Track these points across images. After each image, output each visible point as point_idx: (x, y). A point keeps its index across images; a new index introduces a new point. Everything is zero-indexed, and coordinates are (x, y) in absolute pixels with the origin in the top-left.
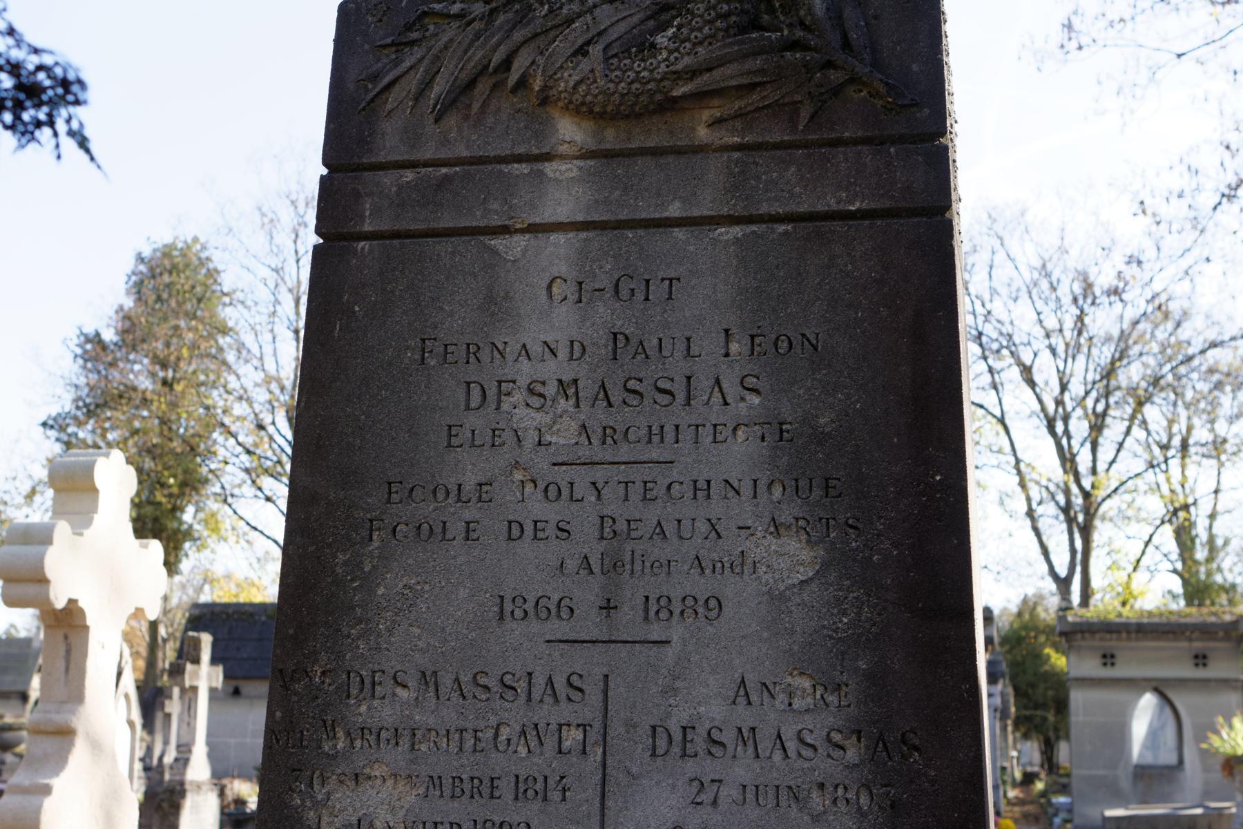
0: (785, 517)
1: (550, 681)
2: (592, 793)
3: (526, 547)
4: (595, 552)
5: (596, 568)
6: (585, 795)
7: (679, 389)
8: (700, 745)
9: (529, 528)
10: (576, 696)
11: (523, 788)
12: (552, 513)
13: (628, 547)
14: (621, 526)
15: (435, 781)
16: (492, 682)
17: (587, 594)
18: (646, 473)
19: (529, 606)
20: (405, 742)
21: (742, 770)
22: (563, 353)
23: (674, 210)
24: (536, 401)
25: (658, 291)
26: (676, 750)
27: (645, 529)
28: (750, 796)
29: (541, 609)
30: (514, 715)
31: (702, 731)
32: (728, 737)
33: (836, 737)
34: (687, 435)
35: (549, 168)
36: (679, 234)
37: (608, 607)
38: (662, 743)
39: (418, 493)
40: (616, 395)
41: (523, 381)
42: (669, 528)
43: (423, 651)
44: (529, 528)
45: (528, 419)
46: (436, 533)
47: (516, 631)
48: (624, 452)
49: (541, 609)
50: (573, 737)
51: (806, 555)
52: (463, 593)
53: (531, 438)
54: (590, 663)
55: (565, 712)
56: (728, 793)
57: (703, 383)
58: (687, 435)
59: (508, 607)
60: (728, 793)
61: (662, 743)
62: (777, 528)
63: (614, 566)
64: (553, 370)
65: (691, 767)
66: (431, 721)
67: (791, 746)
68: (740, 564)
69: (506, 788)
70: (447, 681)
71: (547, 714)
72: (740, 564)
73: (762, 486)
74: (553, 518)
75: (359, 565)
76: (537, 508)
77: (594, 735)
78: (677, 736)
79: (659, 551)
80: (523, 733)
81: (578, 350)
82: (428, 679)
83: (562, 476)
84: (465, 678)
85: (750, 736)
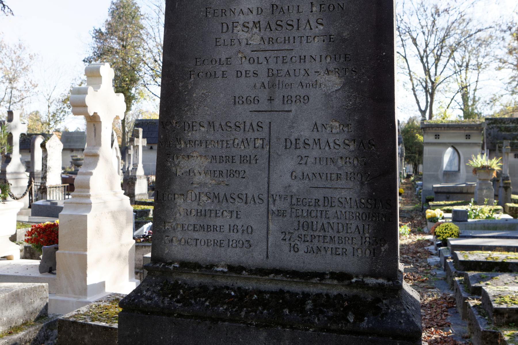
0: (331, 68)
1: (251, 125)
2: (266, 161)
3: (243, 80)
4: (266, 80)
5: (267, 86)
6: (263, 162)
7: (295, 24)
8: (301, 145)
9: (244, 73)
10: (260, 129)
12: (251, 68)
13: (277, 79)
14: (275, 72)
15: (214, 158)
16: (232, 125)
17: (264, 95)
18: (283, 53)
19: (244, 100)
20: (204, 145)
21: (315, 153)
22: (255, 12)
24: (246, 29)
26: (293, 146)
27: (283, 73)
28: (318, 161)
29: (248, 101)
30: (239, 136)
31: (302, 140)
32: (311, 142)
33: (347, 142)
34: (298, 40)
37: (271, 100)
38: (289, 144)
39: (206, 62)
40: (273, 27)
41: (241, 22)
42: (292, 72)
43: (209, 115)
44: (244, 73)
45: (243, 35)
47: (240, 108)
48: (276, 46)
49: (248, 101)
50: (259, 143)
51: (338, 81)
52: (222, 95)
53: (244, 42)
54: (264, 118)
55: (256, 135)
56: (311, 160)
57: (303, 22)
58: (298, 40)
59: (237, 100)
60: (311, 160)
61: (289, 144)
62: (328, 72)
64: (252, 18)
65: (298, 152)
66: (212, 138)
67: (332, 145)
68: (315, 84)
69: (237, 159)
70: (217, 125)
71: (250, 135)
72: (315, 84)
73: (323, 57)
74: (252, 70)
75: (187, 87)
76: (247, 66)
77: (266, 142)
78: (294, 142)
79: (288, 80)
80: (243, 141)
82: (211, 124)
83: (255, 55)
84: (223, 124)
85: (318, 142)
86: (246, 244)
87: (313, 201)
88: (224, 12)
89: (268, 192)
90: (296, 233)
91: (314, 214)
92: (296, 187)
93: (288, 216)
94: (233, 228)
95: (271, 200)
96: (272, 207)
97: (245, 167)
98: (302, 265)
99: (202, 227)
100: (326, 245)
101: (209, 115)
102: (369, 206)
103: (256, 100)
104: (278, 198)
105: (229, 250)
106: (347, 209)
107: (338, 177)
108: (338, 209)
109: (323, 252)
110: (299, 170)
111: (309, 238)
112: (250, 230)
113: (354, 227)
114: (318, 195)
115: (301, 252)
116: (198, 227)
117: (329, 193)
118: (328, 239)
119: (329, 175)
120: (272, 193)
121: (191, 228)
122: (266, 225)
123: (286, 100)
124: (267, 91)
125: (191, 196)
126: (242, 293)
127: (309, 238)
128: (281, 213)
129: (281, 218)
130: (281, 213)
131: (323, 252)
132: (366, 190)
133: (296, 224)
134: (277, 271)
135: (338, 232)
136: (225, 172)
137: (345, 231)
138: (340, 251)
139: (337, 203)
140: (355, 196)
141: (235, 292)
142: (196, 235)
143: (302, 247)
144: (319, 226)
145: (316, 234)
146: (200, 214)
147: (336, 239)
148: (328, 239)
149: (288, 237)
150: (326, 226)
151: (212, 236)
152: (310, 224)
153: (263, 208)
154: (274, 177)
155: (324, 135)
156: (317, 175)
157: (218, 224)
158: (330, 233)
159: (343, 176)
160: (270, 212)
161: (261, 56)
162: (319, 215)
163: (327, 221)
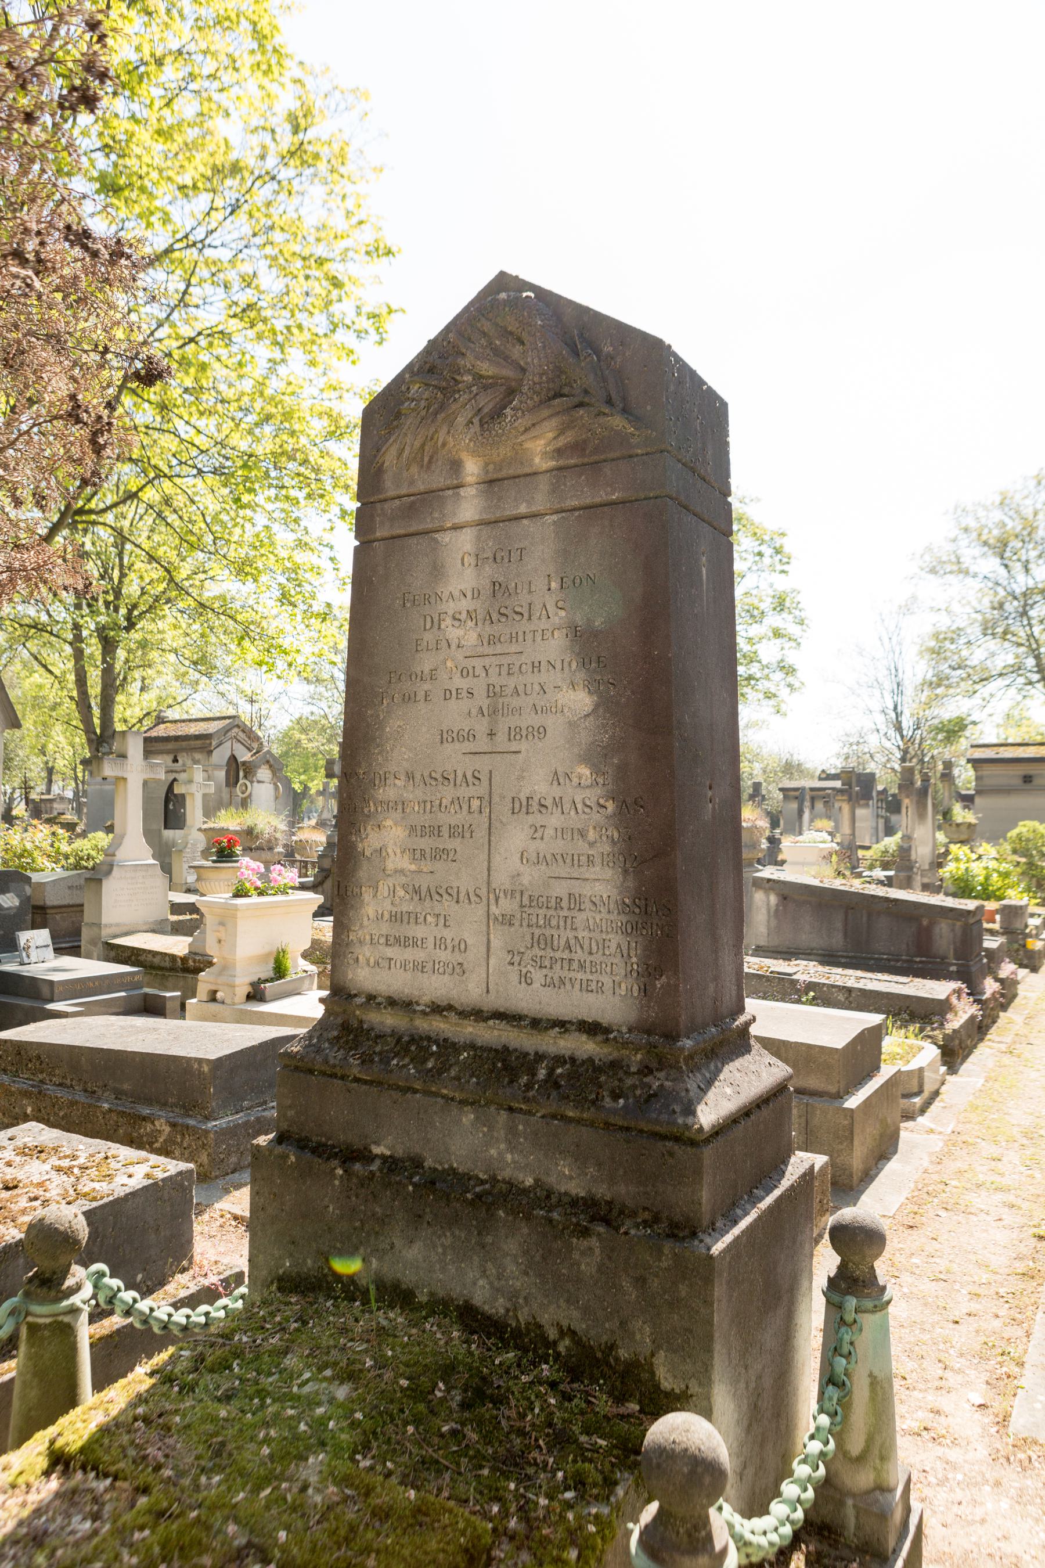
1: (465, 776)
4: (485, 703)
5: (486, 713)
6: (481, 834)
8: (535, 807)
9: (454, 693)
10: (477, 782)
11: (455, 832)
13: (501, 700)
14: (497, 689)
16: (438, 776)
17: (481, 727)
19: (455, 735)
20: (400, 807)
22: (469, 595)
23: (523, 509)
24: (457, 623)
25: (515, 556)
26: (524, 810)
27: (509, 691)
28: (559, 834)
30: (448, 793)
31: (536, 799)
32: (548, 803)
33: (602, 801)
35: (462, 492)
36: (525, 522)
37: (491, 734)
38: (517, 806)
39: (403, 678)
40: (495, 616)
41: (450, 613)
42: (521, 689)
43: (407, 760)
44: (454, 693)
45: (454, 633)
46: (409, 699)
47: (449, 748)
50: (476, 803)
52: (424, 729)
54: (483, 764)
55: (472, 791)
56: (549, 832)
59: (445, 736)
60: (549, 832)
61: (517, 806)
63: (494, 712)
64: (465, 605)
65: (530, 819)
66: (411, 797)
67: (579, 806)
70: (418, 776)
71: (464, 792)
73: (566, 664)
74: (465, 687)
75: (378, 716)
76: (458, 682)
77: (485, 803)
78: (524, 803)
79: (515, 702)
80: (452, 802)
81: (477, 594)
82: (410, 776)
84: (426, 774)
85: (558, 803)
86: (458, 970)
87: (553, 900)
88: (427, 599)
89: (489, 883)
90: (529, 954)
91: (554, 922)
92: (530, 876)
93: (517, 924)
94: (440, 943)
95: (492, 896)
96: (493, 908)
97: (455, 844)
98: (538, 1007)
99: (397, 940)
100: (572, 974)
101: (407, 760)
102: (637, 910)
103: (471, 736)
104: (502, 895)
105: (434, 978)
106: (604, 915)
107: (590, 861)
108: (590, 914)
109: (568, 986)
110: (533, 846)
111: (547, 963)
112: (463, 946)
113: (613, 945)
114: (560, 889)
115: (536, 985)
116: (392, 939)
117: (577, 888)
118: (575, 965)
119: (576, 858)
120: (494, 886)
121: (382, 940)
122: (485, 939)
123: (515, 733)
124: (485, 721)
125: (384, 889)
126: (449, 1047)
127: (547, 963)
128: (507, 920)
129: (506, 927)
130: (507, 920)
131: (568, 986)
132: (630, 884)
133: (528, 937)
134: (500, 1016)
135: (591, 953)
136: (428, 851)
137: (601, 952)
138: (593, 986)
139: (587, 905)
140: (615, 894)
141: (438, 1046)
142: (389, 952)
143: (538, 976)
144: (563, 942)
145: (558, 955)
146: (396, 918)
147: (588, 964)
148: (575, 965)
149: (517, 959)
150: (572, 942)
151: (409, 954)
152: (549, 939)
153: (481, 911)
154: (497, 859)
155: (568, 791)
156: (559, 857)
157: (419, 936)
158: (579, 955)
159: (598, 860)
160: (492, 917)
161: (478, 663)
162: (562, 923)
163: (574, 933)
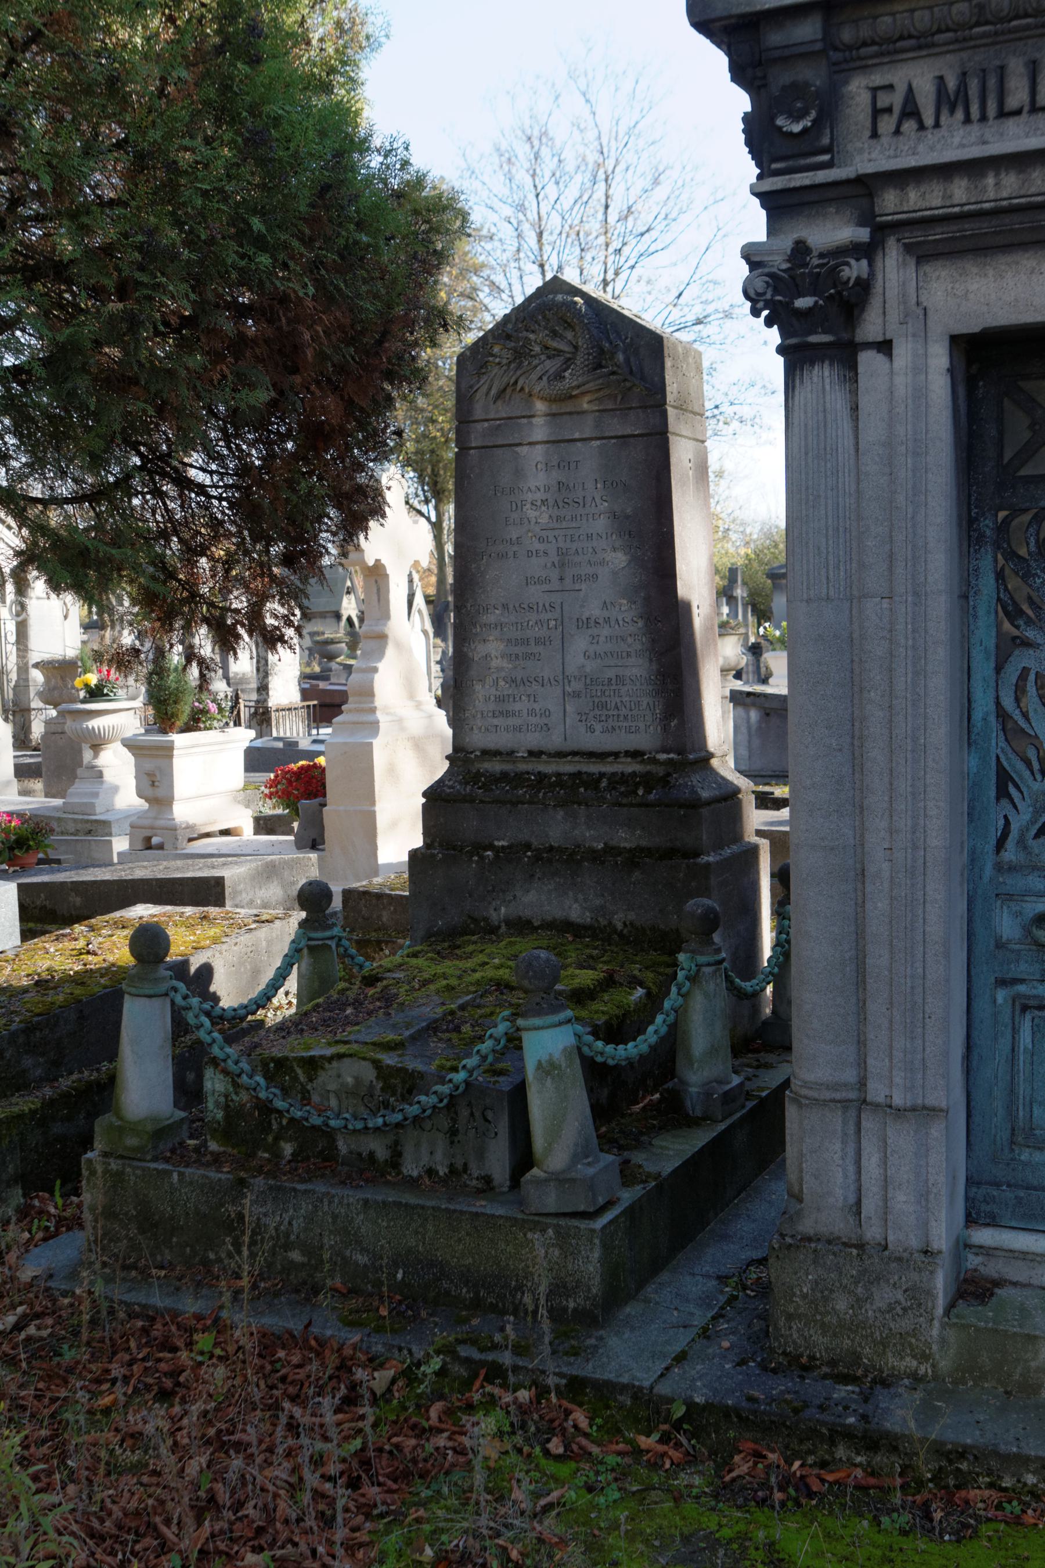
0: (617, 545)
2: (559, 642)
3: (534, 560)
4: (556, 560)
7: (581, 501)
8: (592, 624)
11: (538, 641)
12: (541, 547)
15: (509, 641)
17: (554, 575)
18: (571, 532)
21: (606, 631)
23: (577, 436)
25: (573, 466)
29: (540, 581)
30: (533, 617)
32: (601, 621)
34: (584, 518)
35: (535, 420)
36: (579, 444)
40: (561, 504)
45: (532, 514)
46: (502, 556)
47: (532, 589)
48: (564, 525)
49: (540, 581)
50: (552, 623)
51: (624, 558)
53: (533, 520)
55: (549, 615)
56: (602, 639)
57: (589, 499)
58: (584, 518)
60: (602, 639)
62: (614, 549)
63: (562, 565)
64: (539, 496)
65: (590, 631)
68: (603, 563)
69: (532, 642)
70: (511, 607)
71: (545, 616)
72: (603, 563)
76: (537, 546)
81: (547, 488)
82: (505, 607)
83: (544, 534)
85: (607, 620)
88: (512, 490)
90: (592, 714)
92: (590, 666)
94: (532, 712)
96: (567, 688)
97: (540, 649)
99: (501, 713)
103: (547, 580)
113: (645, 704)
114: (610, 673)
115: (597, 733)
125: (489, 681)
126: (542, 777)
128: (577, 695)
130: (577, 695)
132: (654, 667)
134: (574, 753)
139: (628, 681)
142: (496, 722)
143: (598, 727)
145: (611, 713)
146: (501, 699)
151: (511, 721)
153: (558, 691)
158: (624, 711)
159: (633, 654)
161: (550, 534)
